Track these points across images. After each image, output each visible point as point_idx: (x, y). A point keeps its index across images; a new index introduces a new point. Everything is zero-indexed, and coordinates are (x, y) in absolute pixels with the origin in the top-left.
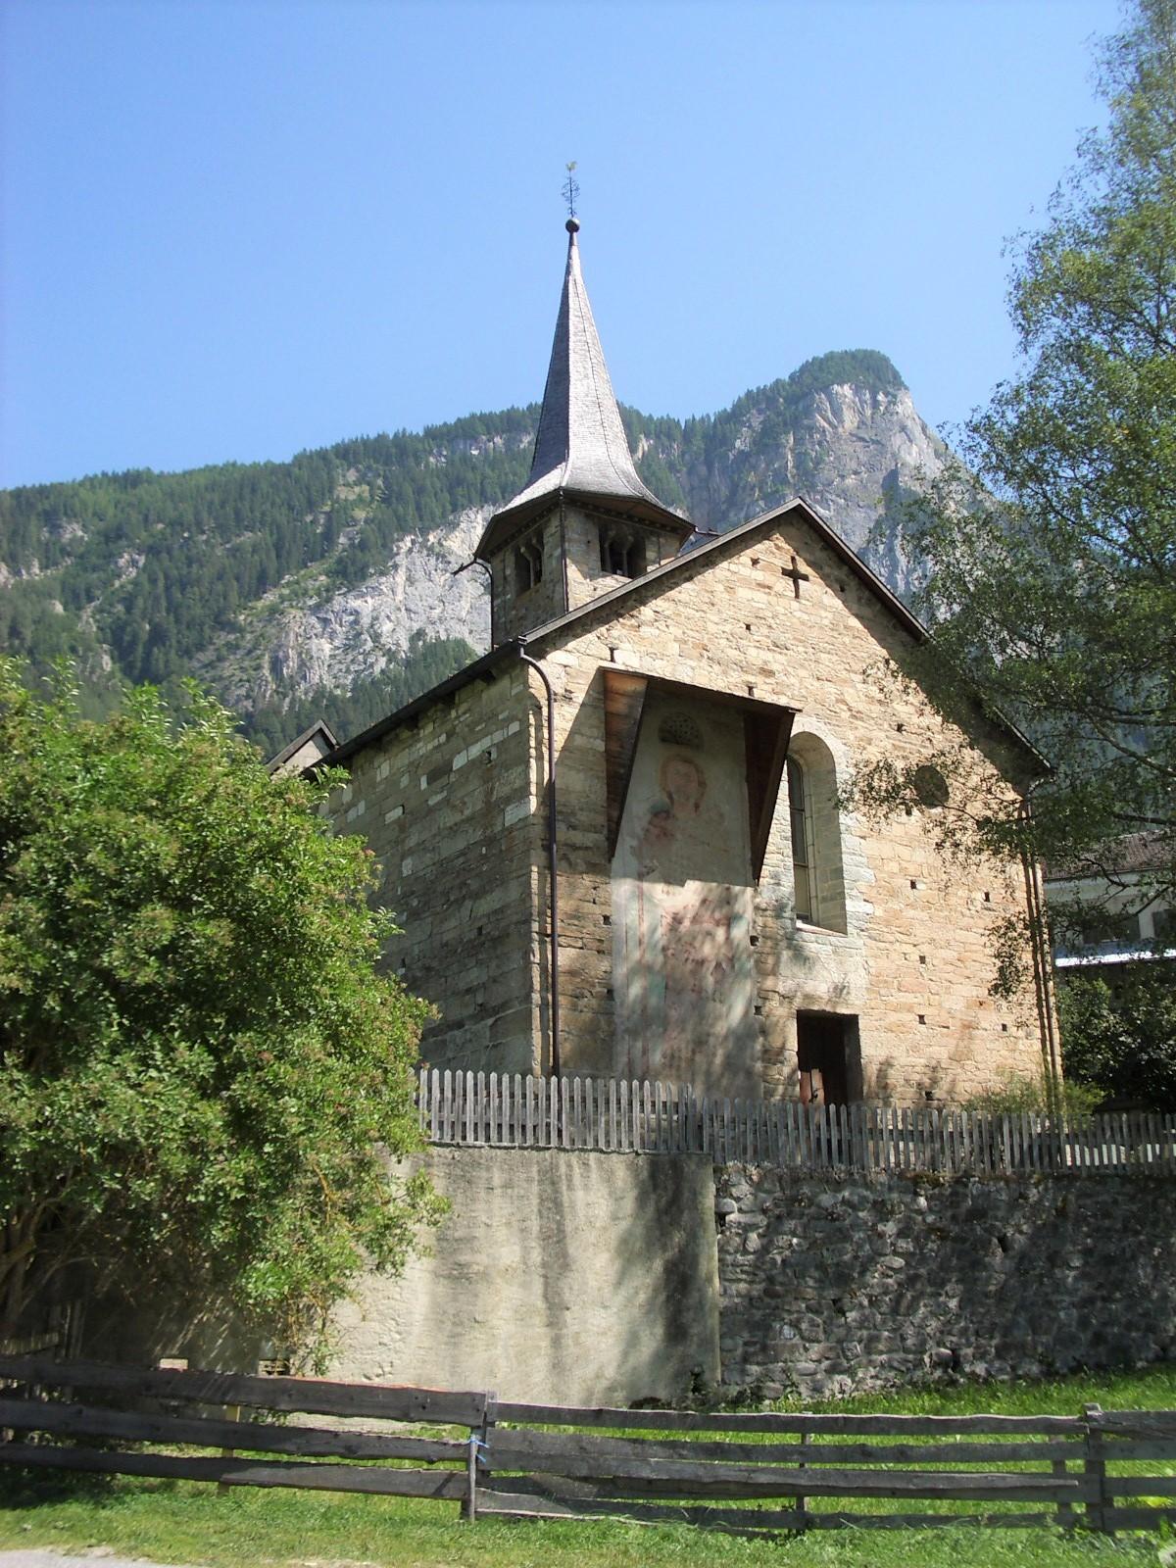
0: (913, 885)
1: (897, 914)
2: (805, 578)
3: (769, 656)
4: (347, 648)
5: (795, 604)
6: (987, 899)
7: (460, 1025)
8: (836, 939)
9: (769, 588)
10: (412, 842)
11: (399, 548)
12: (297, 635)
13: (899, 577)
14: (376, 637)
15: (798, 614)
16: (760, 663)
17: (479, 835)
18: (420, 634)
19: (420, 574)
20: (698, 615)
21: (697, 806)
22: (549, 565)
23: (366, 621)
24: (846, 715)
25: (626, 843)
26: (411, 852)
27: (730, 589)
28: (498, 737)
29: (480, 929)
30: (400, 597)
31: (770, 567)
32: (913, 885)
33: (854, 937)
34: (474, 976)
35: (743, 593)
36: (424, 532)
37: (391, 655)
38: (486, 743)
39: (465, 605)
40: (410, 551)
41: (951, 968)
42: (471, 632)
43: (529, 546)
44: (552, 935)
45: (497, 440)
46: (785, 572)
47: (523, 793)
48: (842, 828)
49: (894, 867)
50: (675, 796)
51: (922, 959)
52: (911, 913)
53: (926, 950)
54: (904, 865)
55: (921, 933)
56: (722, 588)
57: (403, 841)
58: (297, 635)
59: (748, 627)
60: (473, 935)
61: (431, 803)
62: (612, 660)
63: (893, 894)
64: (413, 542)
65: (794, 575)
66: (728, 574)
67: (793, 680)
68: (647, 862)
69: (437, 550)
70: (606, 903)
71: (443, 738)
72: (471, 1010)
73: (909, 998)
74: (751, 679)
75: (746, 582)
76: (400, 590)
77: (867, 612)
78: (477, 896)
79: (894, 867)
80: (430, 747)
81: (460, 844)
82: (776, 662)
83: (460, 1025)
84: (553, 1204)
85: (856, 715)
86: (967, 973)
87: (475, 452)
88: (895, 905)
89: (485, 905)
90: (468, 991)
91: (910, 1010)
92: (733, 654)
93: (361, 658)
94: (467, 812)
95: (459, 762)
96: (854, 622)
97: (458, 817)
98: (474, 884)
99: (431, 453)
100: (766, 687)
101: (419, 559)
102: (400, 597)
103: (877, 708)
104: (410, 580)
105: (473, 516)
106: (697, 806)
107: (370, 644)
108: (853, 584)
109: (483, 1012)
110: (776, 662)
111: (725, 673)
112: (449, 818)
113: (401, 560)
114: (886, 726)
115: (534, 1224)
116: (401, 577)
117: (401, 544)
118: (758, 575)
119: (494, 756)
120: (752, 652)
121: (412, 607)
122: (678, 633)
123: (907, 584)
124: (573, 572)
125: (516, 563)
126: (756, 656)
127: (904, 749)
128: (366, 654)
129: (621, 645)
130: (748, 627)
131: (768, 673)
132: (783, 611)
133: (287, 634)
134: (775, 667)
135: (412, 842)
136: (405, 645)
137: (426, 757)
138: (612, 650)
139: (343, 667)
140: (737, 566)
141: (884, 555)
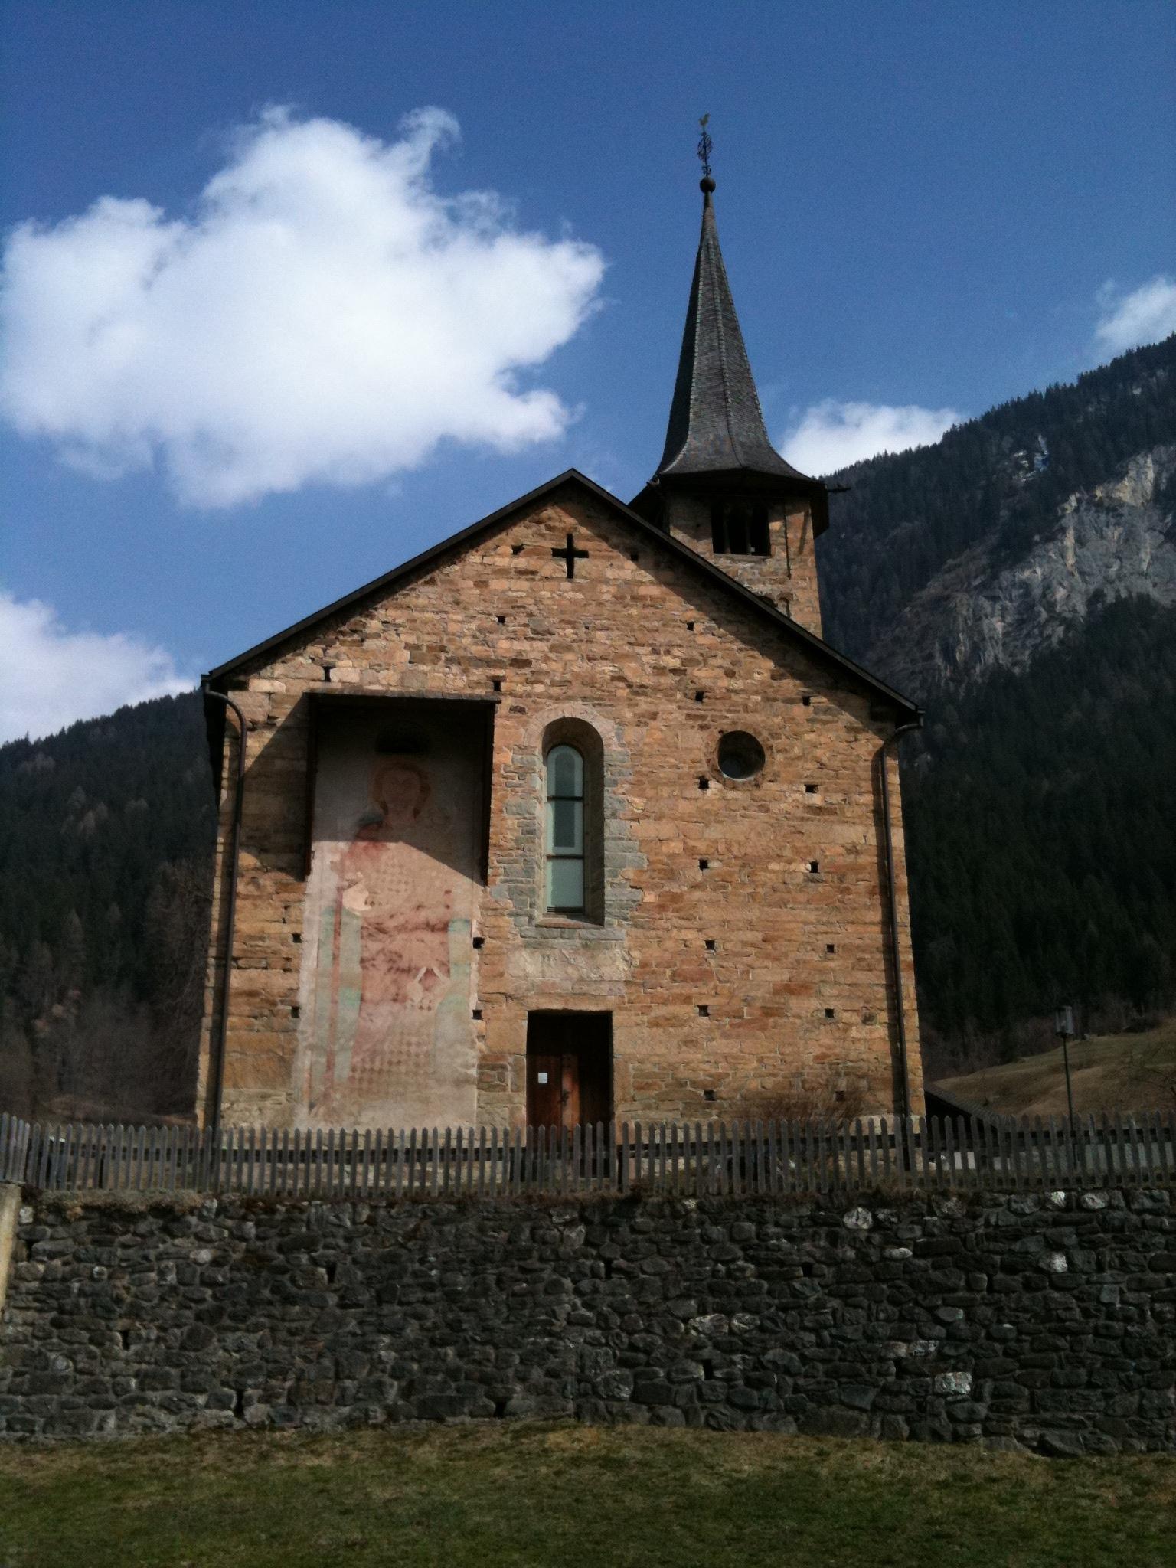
0: (704, 865)
1: (675, 898)
2: (584, 554)
3: (525, 646)
4: (1021, 623)
5: (566, 585)
6: (815, 867)
9: (533, 573)
11: (1064, 510)
12: (966, 619)
14: (1050, 606)
15: (570, 595)
16: (513, 655)
18: (1097, 596)
19: (1092, 534)
20: (437, 617)
21: (416, 813)
23: (1037, 592)
24: (623, 692)
27: (481, 584)
30: (1071, 561)
31: (537, 552)
32: (704, 865)
33: (616, 928)
35: (497, 584)
36: (1090, 487)
37: (1069, 624)
39: (1145, 556)
40: (1077, 510)
41: (753, 951)
42: (1155, 585)
45: (1160, 373)
46: (557, 553)
48: (607, 813)
49: (676, 847)
50: (390, 806)
51: (710, 944)
52: (697, 895)
53: (713, 934)
54: (691, 843)
56: (471, 583)
58: (966, 619)
59: (502, 620)
62: (328, 679)
63: (671, 875)
64: (1079, 501)
65: (569, 554)
66: (480, 568)
67: (554, 666)
68: (350, 876)
69: (1106, 504)
70: (298, 922)
74: (500, 673)
75: (502, 572)
76: (1070, 554)
79: (676, 847)
82: (534, 650)
85: (640, 690)
86: (776, 954)
87: (1137, 392)
91: (687, 1000)
92: (477, 650)
93: (1036, 631)
99: (1088, 402)
100: (518, 678)
101: (1088, 517)
102: (1071, 561)
103: (669, 680)
104: (1080, 541)
105: (1141, 461)
106: (416, 813)
107: (1044, 615)
110: (534, 650)
111: (465, 671)
113: (1069, 522)
114: (679, 696)
116: (1069, 540)
117: (1066, 506)
118: (521, 562)
121: (1086, 569)
122: (412, 639)
126: (505, 647)
127: (703, 717)
128: (1042, 627)
129: (339, 663)
130: (502, 620)
131: (520, 662)
132: (548, 594)
133: (955, 619)
134: (531, 656)
136: (1082, 609)
138: (327, 670)
139: (1019, 643)
140: (498, 554)
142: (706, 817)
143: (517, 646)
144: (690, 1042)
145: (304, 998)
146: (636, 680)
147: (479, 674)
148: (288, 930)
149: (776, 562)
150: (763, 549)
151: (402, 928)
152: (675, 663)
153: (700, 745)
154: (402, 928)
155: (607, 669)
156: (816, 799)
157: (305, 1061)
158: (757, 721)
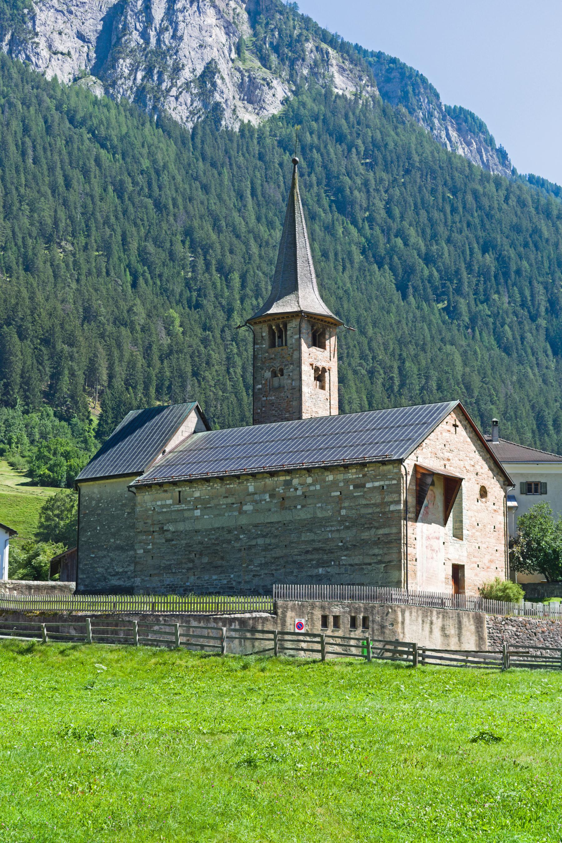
7: (370, 564)
8: (460, 542)
10: (346, 504)
13: (152, 33)
17: (378, 510)
22: (291, 341)
25: (420, 516)
26: (344, 508)
28: (387, 483)
29: (379, 538)
33: (465, 541)
34: (376, 551)
38: (382, 483)
43: (278, 326)
44: (407, 544)
47: (398, 502)
53: (480, 545)
55: (479, 540)
57: (341, 504)
60: (376, 539)
61: (355, 494)
65: (455, 426)
71: (361, 476)
72: (375, 561)
73: (474, 559)
77: (471, 435)
78: (377, 528)
79: (474, 519)
80: (354, 476)
81: (370, 511)
83: (370, 564)
84: (460, 623)
88: (474, 531)
89: (381, 532)
90: (374, 555)
94: (372, 502)
95: (369, 485)
96: (469, 440)
97: (368, 502)
98: (376, 524)
103: (472, 468)
108: (468, 426)
109: (380, 562)
112: (364, 502)
115: (456, 626)
119: (385, 488)
120: (446, 453)
123: (159, 41)
124: (304, 347)
125: (269, 332)
126: (447, 455)
134: (450, 458)
135: (346, 504)
137: (353, 480)
141: (140, 12)
142: (478, 511)
143: (449, 454)
144: (476, 575)
145: (417, 557)
146: (468, 468)
147: (443, 462)
148: (414, 536)
149: (327, 353)
150: (322, 346)
151: (432, 538)
152: (473, 464)
153: (477, 489)
154: (432, 538)
155: (462, 463)
156: (495, 507)
157: (419, 574)
158: (487, 484)
